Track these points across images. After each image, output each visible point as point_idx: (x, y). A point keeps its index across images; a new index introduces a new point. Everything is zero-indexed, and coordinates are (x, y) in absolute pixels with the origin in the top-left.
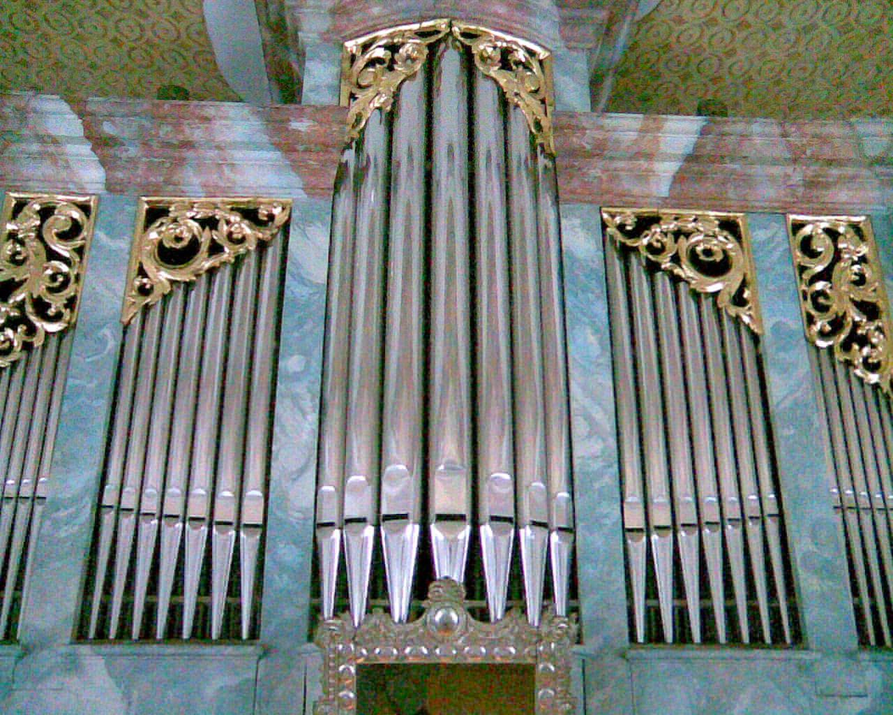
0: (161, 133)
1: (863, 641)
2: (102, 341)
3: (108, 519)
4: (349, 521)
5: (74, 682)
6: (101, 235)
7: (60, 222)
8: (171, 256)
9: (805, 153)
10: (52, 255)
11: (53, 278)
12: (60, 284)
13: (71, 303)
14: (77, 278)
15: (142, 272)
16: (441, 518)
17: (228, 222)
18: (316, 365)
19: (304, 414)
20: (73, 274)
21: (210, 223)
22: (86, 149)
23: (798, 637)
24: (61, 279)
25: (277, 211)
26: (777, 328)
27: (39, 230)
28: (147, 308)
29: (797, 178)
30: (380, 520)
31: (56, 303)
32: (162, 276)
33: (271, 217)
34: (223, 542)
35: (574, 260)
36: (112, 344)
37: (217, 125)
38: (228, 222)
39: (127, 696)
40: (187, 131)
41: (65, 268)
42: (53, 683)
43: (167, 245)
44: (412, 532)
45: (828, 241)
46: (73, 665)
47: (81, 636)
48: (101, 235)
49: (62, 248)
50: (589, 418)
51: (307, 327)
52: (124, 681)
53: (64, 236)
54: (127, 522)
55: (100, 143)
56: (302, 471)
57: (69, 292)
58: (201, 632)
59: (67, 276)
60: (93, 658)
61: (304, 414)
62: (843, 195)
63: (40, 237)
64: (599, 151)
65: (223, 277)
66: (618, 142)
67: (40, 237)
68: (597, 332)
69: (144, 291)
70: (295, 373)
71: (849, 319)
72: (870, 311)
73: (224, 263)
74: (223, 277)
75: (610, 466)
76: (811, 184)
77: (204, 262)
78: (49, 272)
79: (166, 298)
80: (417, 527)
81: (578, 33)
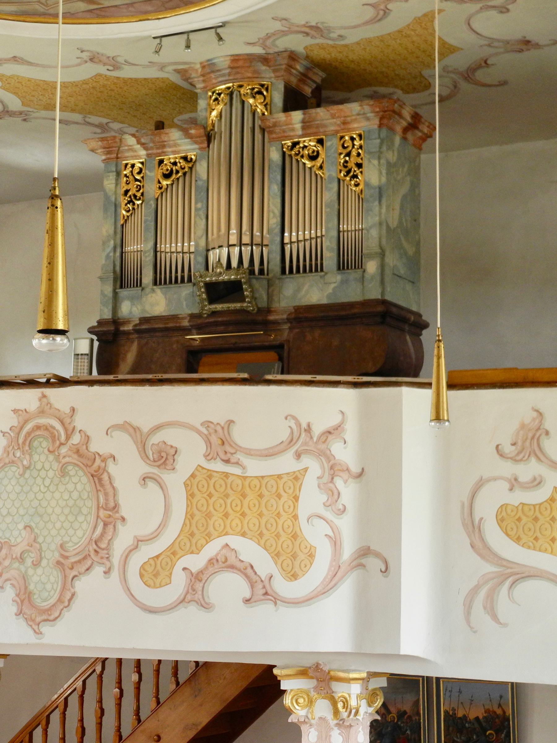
0: (156, 139)
1: (339, 269)
2: (151, 205)
3: (158, 254)
4: (178, 252)
5: (154, 295)
6: (147, 172)
7: (136, 170)
8: (167, 176)
9: (335, 115)
10: (137, 180)
11: (137, 187)
12: (139, 188)
13: (142, 194)
14: (143, 186)
15: (159, 182)
16: (256, 245)
17: (180, 163)
18: (205, 206)
19: (202, 220)
20: (142, 185)
21: (175, 164)
22: (139, 146)
23: (322, 270)
24: (139, 187)
25: (193, 157)
26: (330, 176)
27: (132, 172)
28: (162, 193)
29: (339, 122)
30: (229, 246)
31: (139, 194)
32: (165, 183)
33: (191, 159)
34: (187, 256)
35: (273, 161)
36: (153, 206)
37: (171, 135)
38: (180, 163)
39: (166, 297)
40: (163, 138)
41: (139, 183)
42: (150, 295)
43: (164, 173)
44: (237, 249)
45: (350, 142)
46: (153, 291)
47: (155, 283)
48: (147, 172)
49: (138, 177)
50: (273, 212)
51: (202, 194)
52: (165, 294)
53: (139, 173)
54: (163, 255)
55: (143, 144)
56: (202, 236)
57: (141, 191)
58: (183, 281)
59: (140, 186)
60: (158, 290)
61: (202, 220)
62: (355, 125)
63: (132, 175)
64: (275, 125)
65: (181, 180)
66: (280, 121)
67: (132, 175)
68: (277, 184)
69: (160, 188)
70: (199, 208)
71: (353, 169)
72: (359, 166)
73: (180, 177)
74: (181, 180)
75: (278, 226)
76: (344, 123)
77: (174, 176)
78: (135, 186)
79: (167, 189)
80: (239, 247)
81: (278, 74)
